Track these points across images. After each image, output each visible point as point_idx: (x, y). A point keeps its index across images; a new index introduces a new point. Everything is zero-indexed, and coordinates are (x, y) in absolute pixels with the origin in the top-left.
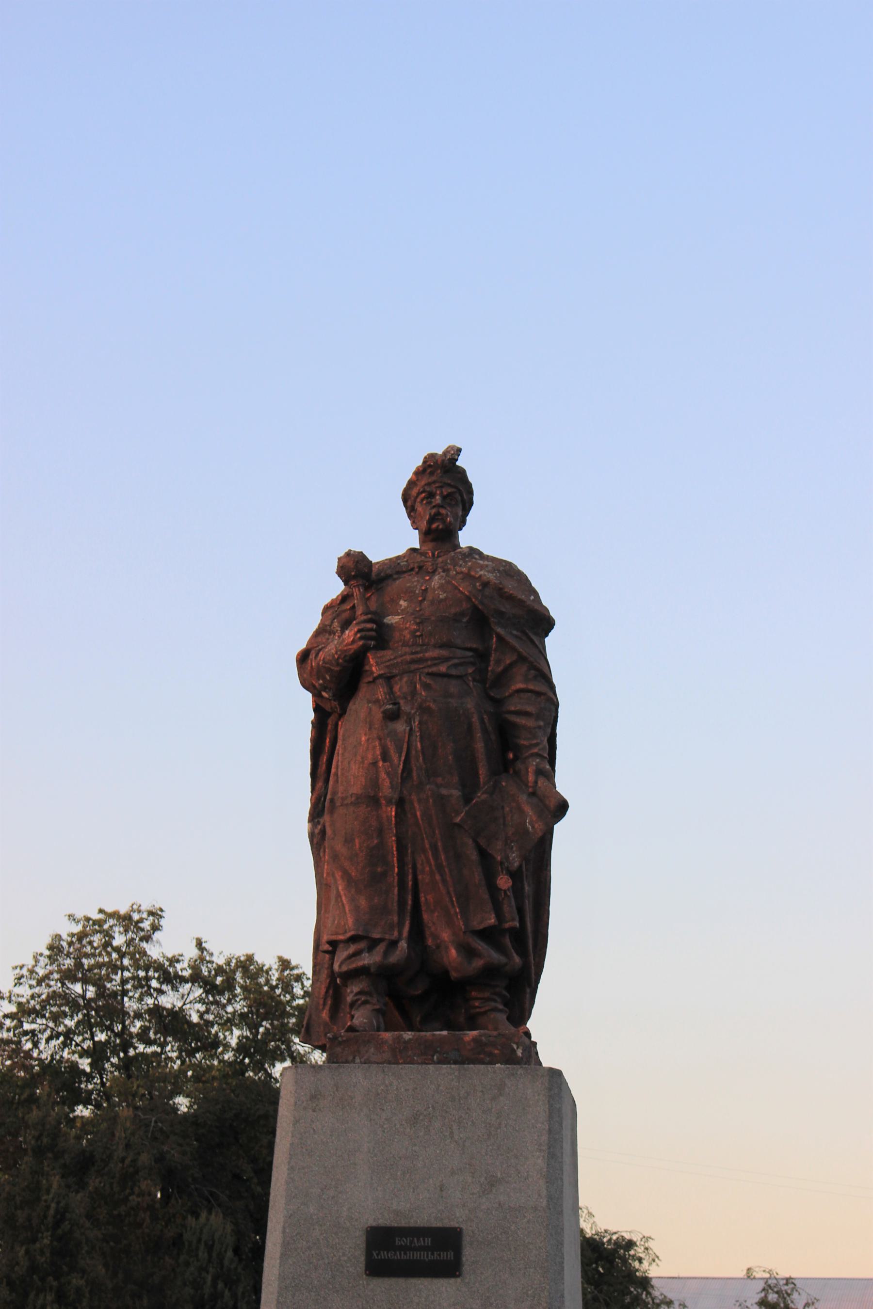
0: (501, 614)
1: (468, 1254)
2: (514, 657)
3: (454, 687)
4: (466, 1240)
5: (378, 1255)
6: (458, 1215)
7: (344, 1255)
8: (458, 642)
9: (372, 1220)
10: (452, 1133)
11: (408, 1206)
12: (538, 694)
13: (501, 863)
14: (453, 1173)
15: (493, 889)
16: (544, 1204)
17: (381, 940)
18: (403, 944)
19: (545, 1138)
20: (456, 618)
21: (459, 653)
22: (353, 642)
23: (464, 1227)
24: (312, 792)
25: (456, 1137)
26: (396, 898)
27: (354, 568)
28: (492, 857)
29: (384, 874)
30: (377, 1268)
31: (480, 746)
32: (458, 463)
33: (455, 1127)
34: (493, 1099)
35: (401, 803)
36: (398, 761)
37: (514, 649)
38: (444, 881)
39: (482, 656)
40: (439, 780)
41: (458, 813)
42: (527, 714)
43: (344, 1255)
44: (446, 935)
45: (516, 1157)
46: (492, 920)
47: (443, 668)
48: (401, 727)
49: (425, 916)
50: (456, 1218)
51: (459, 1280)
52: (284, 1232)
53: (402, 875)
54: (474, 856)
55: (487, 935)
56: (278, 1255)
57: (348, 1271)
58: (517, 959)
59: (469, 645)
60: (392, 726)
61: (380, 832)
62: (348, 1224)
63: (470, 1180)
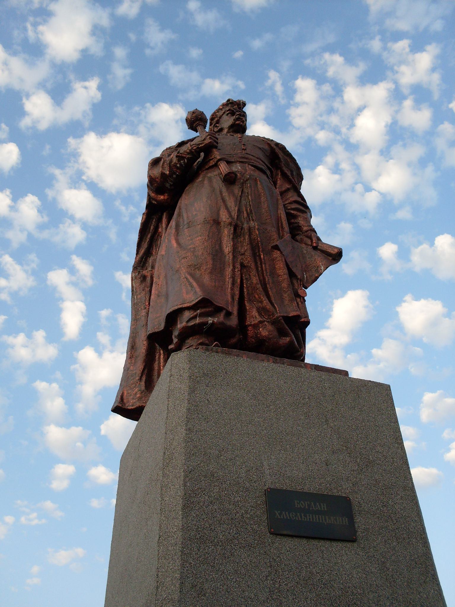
1: (360, 521)
4: (356, 508)
5: (280, 514)
6: (344, 487)
7: (247, 512)
9: (270, 481)
11: (301, 474)
22: (205, 139)
23: (350, 497)
24: (137, 254)
30: (277, 530)
43: (247, 512)
49: (247, 304)
50: (344, 489)
51: (355, 544)
52: (185, 485)
56: (179, 507)
57: (252, 528)
62: (248, 485)
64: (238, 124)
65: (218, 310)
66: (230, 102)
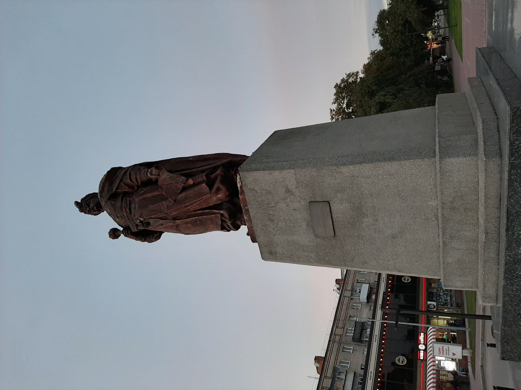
0: (108, 191)
2: (122, 183)
3: (133, 206)
4: (313, 200)
8: (120, 204)
10: (273, 207)
12: (130, 175)
13: (184, 184)
14: (288, 206)
15: (195, 185)
16: (292, 170)
17: (221, 220)
18: (222, 212)
19: (266, 172)
20: (113, 206)
21: (123, 204)
23: (308, 201)
25: (274, 205)
26: (207, 216)
27: (114, 234)
28: (183, 187)
29: (200, 220)
31: (149, 195)
32: (80, 201)
33: (270, 206)
34: (257, 192)
35: (174, 219)
36: (161, 221)
37: (119, 183)
38: (196, 202)
39: (125, 194)
40: (162, 208)
41: (171, 202)
42: (136, 178)
44: (214, 198)
45: (276, 182)
46: (204, 185)
47: (128, 210)
48: (151, 221)
53: (199, 215)
54: (183, 194)
55: (210, 185)
58: (219, 171)
59: (120, 200)
60: (151, 224)
61: (187, 223)
63: (289, 200)
64: (97, 209)
65: (223, 221)
66: (81, 211)
